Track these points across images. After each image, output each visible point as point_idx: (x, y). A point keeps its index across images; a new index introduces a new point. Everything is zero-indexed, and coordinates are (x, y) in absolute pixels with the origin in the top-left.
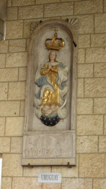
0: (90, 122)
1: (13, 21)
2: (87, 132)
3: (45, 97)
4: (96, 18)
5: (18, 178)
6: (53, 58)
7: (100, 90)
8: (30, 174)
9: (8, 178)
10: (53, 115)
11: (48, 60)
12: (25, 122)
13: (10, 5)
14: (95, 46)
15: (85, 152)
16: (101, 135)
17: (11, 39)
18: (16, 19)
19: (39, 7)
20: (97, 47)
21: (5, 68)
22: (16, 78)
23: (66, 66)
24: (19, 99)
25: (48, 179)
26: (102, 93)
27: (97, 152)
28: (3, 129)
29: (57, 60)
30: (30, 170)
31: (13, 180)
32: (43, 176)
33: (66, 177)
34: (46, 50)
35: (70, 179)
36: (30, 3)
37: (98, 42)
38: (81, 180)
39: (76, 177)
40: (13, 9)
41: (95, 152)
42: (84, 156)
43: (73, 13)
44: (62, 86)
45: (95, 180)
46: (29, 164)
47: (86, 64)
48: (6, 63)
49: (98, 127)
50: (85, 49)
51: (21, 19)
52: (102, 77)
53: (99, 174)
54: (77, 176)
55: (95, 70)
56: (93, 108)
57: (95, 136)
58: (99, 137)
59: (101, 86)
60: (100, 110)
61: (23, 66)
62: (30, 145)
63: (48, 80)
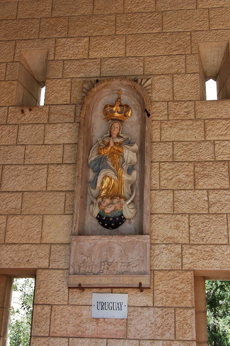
0: (170, 224)
1: (56, 80)
2: (165, 239)
3: (103, 187)
4: (175, 80)
5: (62, 307)
6: (115, 132)
7: (183, 179)
8: (78, 300)
9: (45, 306)
10: (117, 214)
11: (108, 134)
12: (75, 221)
13: (52, 58)
14: (175, 118)
15: (163, 268)
16: (186, 244)
17: (53, 104)
18: (60, 76)
19: (94, 62)
20: (177, 120)
21: (44, 144)
22: (59, 160)
23: (134, 143)
24: (64, 189)
25: (106, 309)
26: (186, 183)
27: (181, 268)
28: (39, 233)
29: (121, 135)
30: (79, 295)
31: (53, 310)
32: (99, 303)
33: (134, 305)
34: (104, 121)
35: (140, 309)
36: (80, 56)
37: (179, 113)
38: (156, 311)
39: (149, 305)
40: (56, 63)
41: (178, 269)
42: (161, 274)
43: (143, 72)
44: (129, 172)
45: (178, 311)
46: (80, 285)
47: (162, 142)
48: (46, 138)
49: (181, 231)
50: (161, 122)
51: (67, 77)
52: (185, 162)
53: (185, 302)
54: (150, 304)
55: (175, 149)
56: (173, 205)
57: (177, 246)
58: (183, 246)
59: (184, 173)
60: (183, 208)
61: (70, 143)
62: (81, 256)
63: (108, 163)
